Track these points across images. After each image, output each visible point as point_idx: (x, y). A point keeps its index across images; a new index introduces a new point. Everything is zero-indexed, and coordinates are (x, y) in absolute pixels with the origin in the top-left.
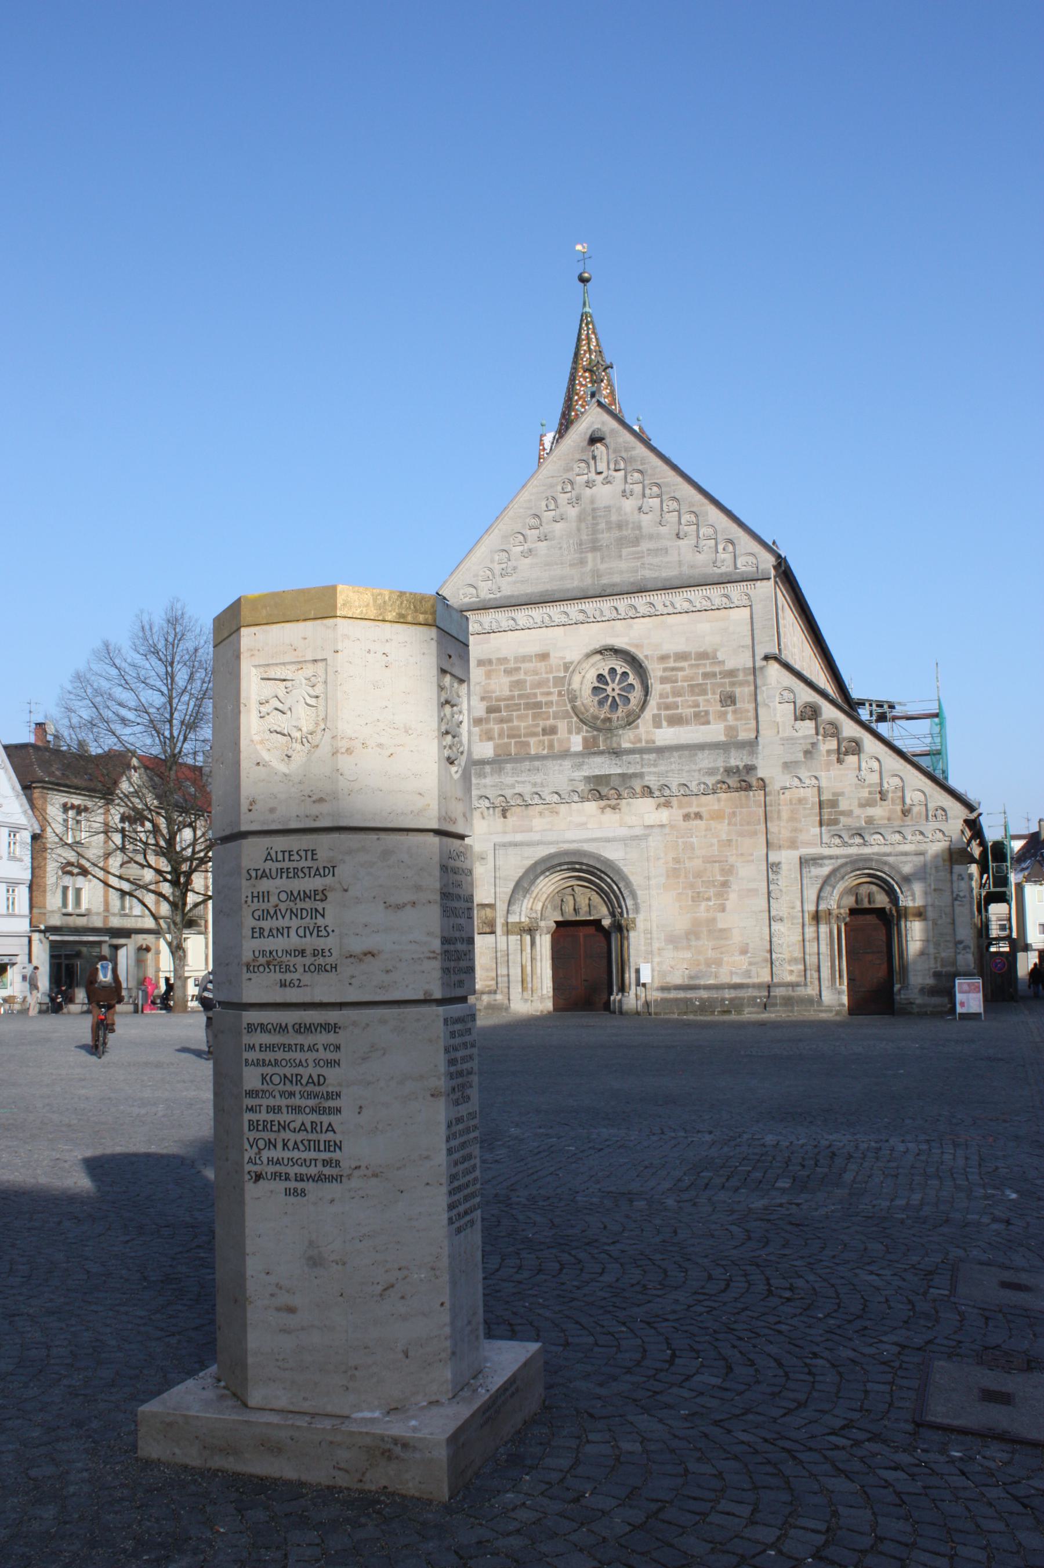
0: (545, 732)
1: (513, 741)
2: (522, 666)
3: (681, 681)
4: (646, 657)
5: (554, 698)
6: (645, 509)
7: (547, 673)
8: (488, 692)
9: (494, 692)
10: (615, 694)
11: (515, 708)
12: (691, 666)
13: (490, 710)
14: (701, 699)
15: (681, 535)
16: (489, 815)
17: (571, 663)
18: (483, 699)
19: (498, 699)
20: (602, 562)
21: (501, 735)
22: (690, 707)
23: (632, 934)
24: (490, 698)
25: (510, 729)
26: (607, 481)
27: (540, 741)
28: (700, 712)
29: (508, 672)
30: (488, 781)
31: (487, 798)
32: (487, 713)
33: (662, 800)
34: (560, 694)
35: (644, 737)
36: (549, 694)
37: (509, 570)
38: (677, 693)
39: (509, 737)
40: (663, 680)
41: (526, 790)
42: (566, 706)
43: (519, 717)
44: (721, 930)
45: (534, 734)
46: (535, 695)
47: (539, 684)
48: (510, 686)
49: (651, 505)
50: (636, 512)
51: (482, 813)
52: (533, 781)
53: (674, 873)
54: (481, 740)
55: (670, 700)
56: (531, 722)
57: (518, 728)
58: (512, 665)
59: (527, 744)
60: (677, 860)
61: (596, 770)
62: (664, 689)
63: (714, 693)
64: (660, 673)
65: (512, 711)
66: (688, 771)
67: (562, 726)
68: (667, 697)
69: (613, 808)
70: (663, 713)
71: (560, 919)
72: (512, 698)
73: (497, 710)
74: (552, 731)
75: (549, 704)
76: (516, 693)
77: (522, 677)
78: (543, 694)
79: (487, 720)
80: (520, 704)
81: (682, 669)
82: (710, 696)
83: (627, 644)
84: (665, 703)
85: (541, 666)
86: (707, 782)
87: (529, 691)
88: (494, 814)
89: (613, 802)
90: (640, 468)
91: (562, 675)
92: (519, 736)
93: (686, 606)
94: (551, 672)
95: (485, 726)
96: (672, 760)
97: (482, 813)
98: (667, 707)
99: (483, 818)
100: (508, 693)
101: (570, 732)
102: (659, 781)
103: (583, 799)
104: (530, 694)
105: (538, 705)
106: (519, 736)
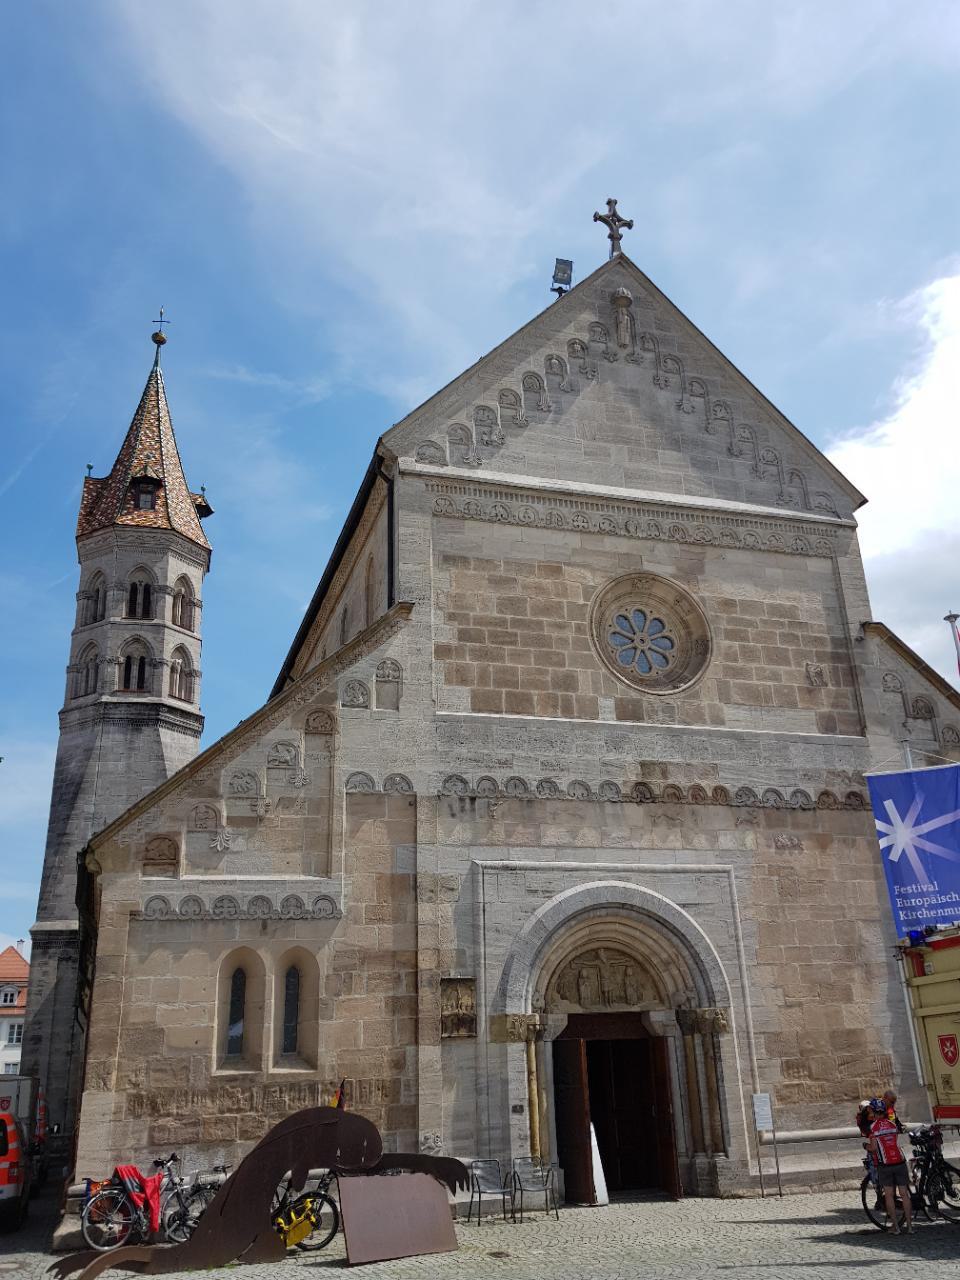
0: (557, 685)
1: (504, 690)
2: (520, 578)
3: (753, 640)
4: (703, 599)
5: (570, 634)
6: (686, 406)
7: (558, 595)
8: (462, 608)
9: (473, 609)
10: (640, 646)
11: (507, 639)
12: (764, 622)
13: (463, 635)
14: (782, 669)
15: (735, 450)
16: (463, 810)
17: (594, 587)
18: (451, 617)
19: (479, 621)
20: (630, 460)
21: (483, 678)
22: (765, 678)
23: (724, 1039)
24: (465, 618)
25: (505, 670)
26: (633, 359)
27: (549, 696)
28: (785, 687)
29: (497, 582)
30: (463, 751)
31: (464, 782)
32: (460, 639)
33: (743, 813)
34: (579, 629)
35: (707, 712)
36: (561, 627)
37: (494, 438)
38: (749, 654)
39: (498, 683)
40: (731, 635)
41: (533, 777)
42: (589, 650)
43: (516, 656)
44: (851, 1032)
45: (542, 685)
46: (540, 624)
47: (547, 610)
48: (498, 605)
49: (694, 404)
50: (673, 408)
51: (450, 807)
52: (542, 759)
53: (770, 931)
54: (448, 681)
55: (740, 664)
56: (533, 666)
57: (514, 671)
58: (501, 572)
59: (528, 699)
60: (772, 910)
61: (645, 753)
62: (730, 647)
63: (799, 664)
64: (724, 625)
65: (503, 643)
66: (780, 771)
67: (584, 677)
68: (736, 660)
69: (671, 821)
70: (732, 681)
71: (578, 1009)
72: (502, 623)
73: (479, 638)
74: (568, 682)
75: (563, 642)
76: (509, 617)
77: (518, 592)
78: (550, 625)
79: (459, 652)
80: (516, 635)
81: (750, 624)
82: (793, 668)
83: (673, 576)
84: (732, 668)
85: (547, 582)
86: (808, 790)
87: (529, 617)
88: (473, 810)
89: (671, 809)
90: (677, 354)
91: (581, 602)
92: (515, 685)
93: (750, 540)
94: (565, 595)
95: (453, 661)
96: (753, 751)
97: (450, 807)
98: (737, 673)
99: (453, 815)
100: (496, 614)
101: (596, 690)
102: (738, 780)
103: (628, 799)
104: (531, 622)
105: (541, 641)
106: (515, 685)
